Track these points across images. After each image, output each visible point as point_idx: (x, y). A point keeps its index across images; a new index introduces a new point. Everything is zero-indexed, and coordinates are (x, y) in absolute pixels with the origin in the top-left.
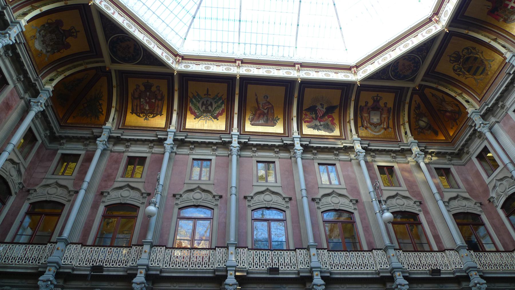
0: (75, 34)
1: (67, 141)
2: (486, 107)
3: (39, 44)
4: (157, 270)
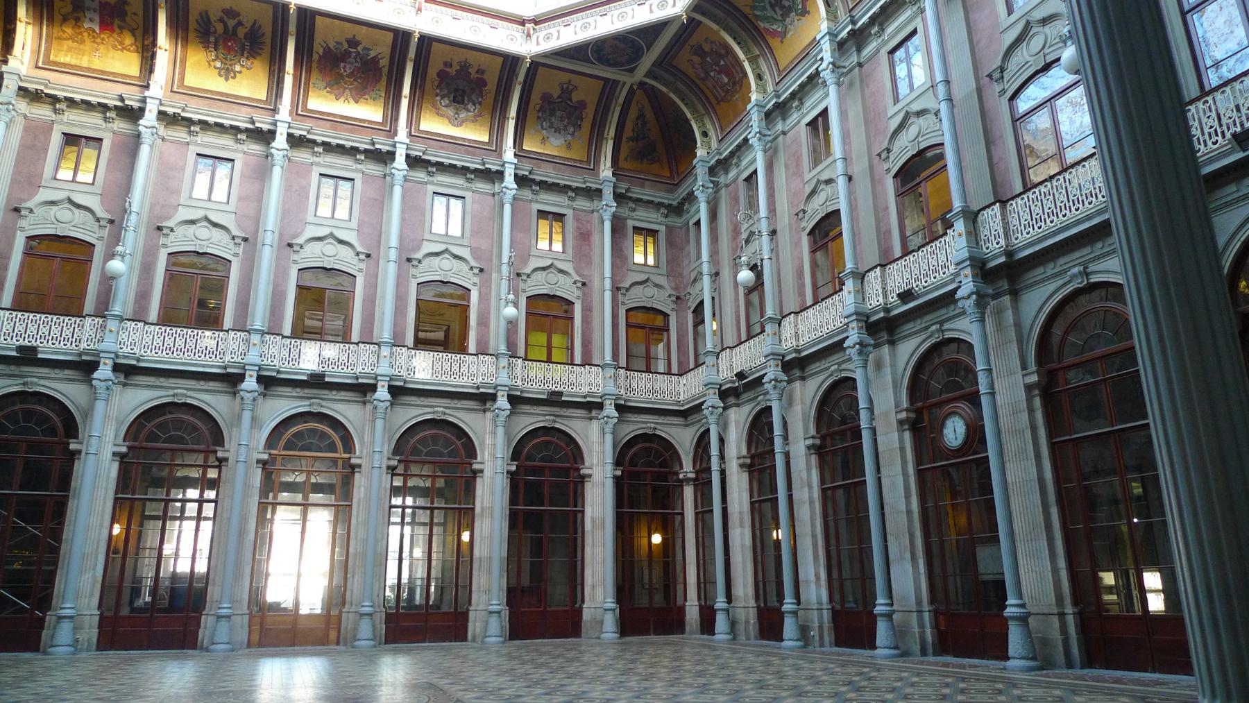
0: (571, 87)
1: (690, 203)
3: (556, 138)
4: (790, 353)
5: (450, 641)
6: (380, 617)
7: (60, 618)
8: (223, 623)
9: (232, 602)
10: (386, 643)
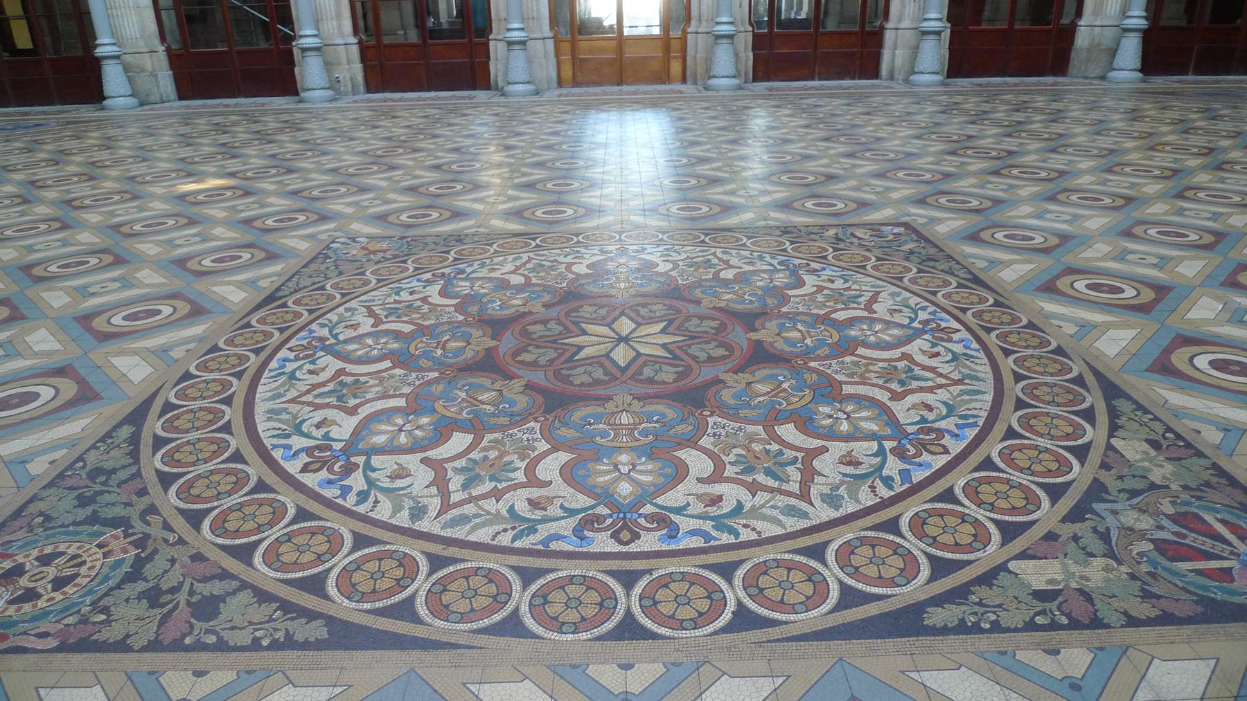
5: (853, 78)
6: (745, 40)
7: (304, 50)
8: (516, 52)
9: (523, 20)
10: (755, 80)
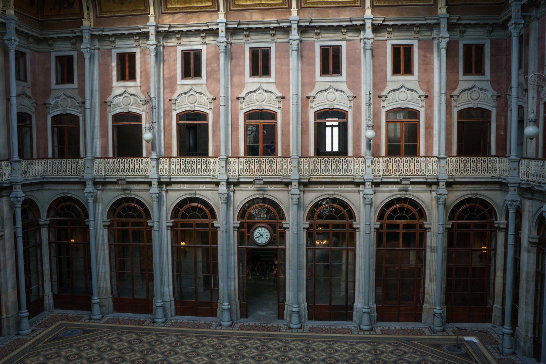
2: (101, 33)
